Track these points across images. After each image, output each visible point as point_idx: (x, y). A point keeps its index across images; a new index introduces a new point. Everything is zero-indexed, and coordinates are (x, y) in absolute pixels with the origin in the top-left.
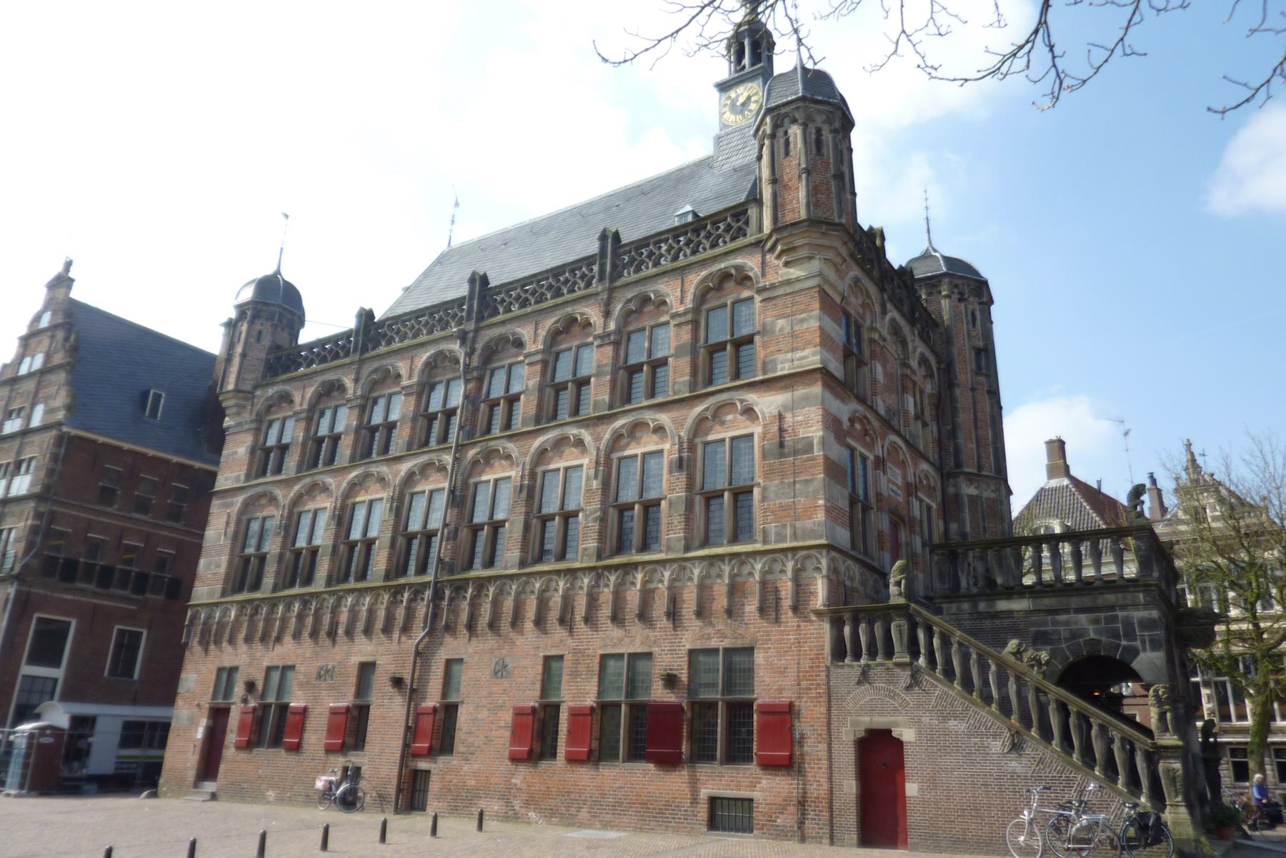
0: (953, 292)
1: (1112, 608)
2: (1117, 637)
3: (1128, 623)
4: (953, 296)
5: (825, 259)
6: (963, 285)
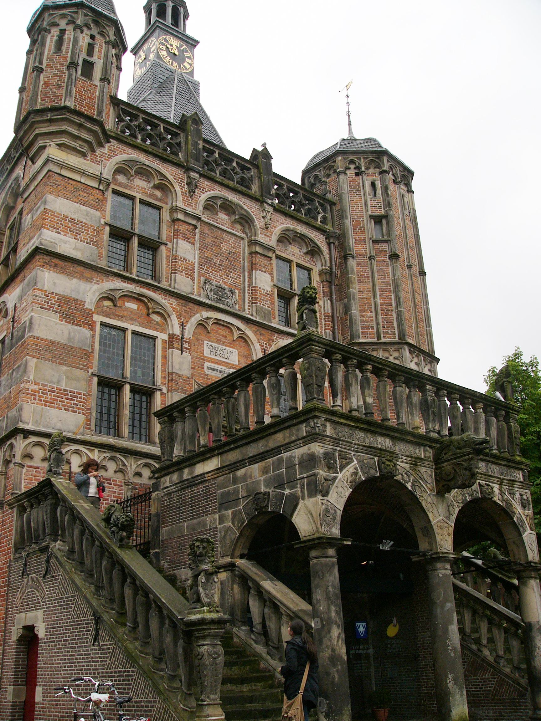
0: (349, 168)
1: (277, 450)
2: (281, 486)
3: (290, 466)
4: (348, 172)
5: (57, 145)
6: (359, 159)
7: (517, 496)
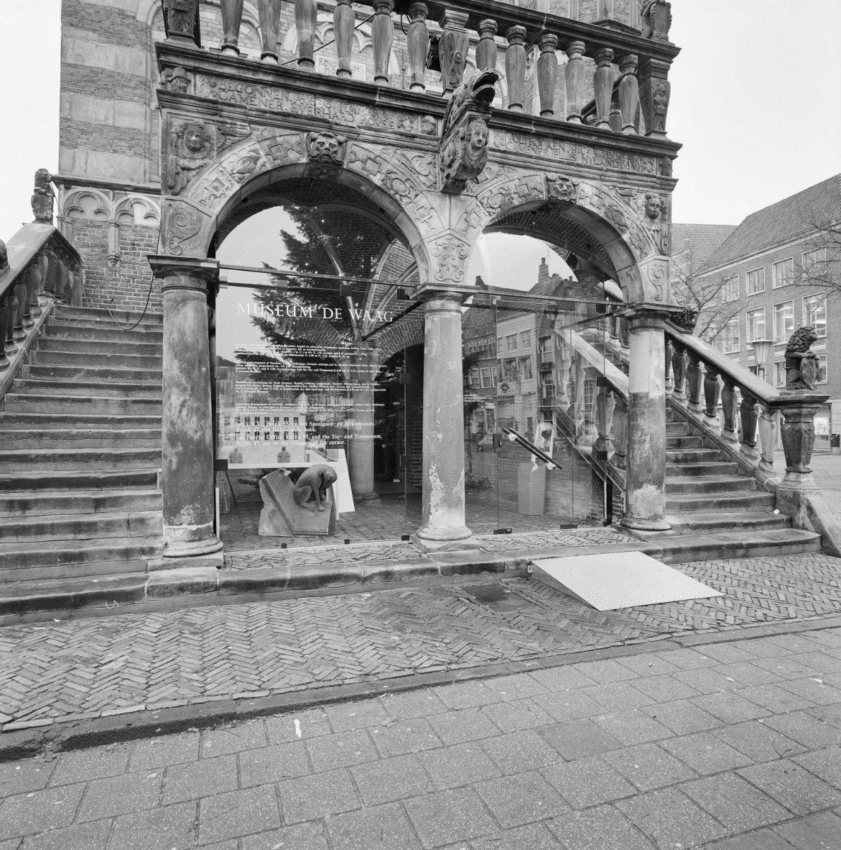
7: (641, 200)
